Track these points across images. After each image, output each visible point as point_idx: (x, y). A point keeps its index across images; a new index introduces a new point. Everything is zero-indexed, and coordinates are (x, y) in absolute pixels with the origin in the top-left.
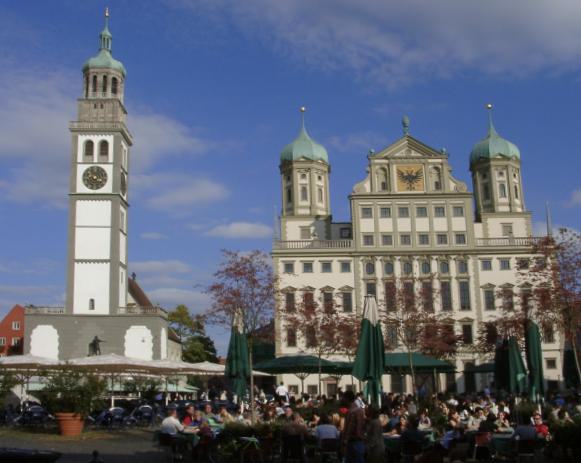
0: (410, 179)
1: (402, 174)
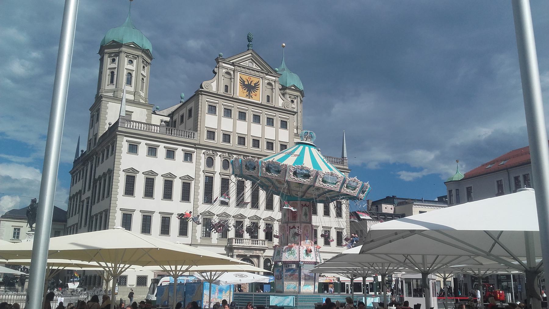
0: (250, 88)
1: (244, 82)
